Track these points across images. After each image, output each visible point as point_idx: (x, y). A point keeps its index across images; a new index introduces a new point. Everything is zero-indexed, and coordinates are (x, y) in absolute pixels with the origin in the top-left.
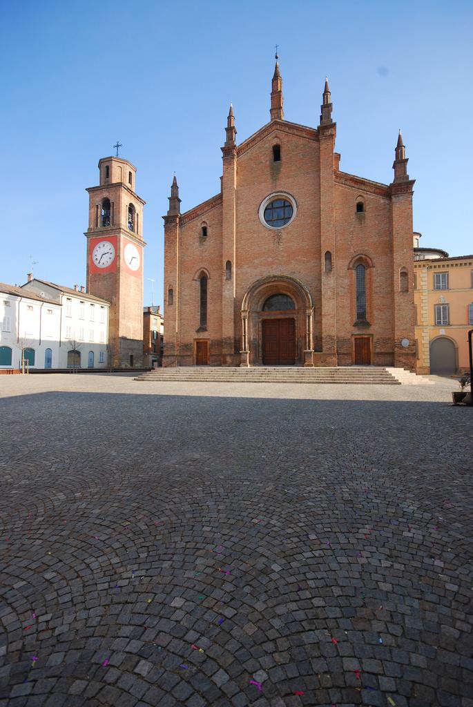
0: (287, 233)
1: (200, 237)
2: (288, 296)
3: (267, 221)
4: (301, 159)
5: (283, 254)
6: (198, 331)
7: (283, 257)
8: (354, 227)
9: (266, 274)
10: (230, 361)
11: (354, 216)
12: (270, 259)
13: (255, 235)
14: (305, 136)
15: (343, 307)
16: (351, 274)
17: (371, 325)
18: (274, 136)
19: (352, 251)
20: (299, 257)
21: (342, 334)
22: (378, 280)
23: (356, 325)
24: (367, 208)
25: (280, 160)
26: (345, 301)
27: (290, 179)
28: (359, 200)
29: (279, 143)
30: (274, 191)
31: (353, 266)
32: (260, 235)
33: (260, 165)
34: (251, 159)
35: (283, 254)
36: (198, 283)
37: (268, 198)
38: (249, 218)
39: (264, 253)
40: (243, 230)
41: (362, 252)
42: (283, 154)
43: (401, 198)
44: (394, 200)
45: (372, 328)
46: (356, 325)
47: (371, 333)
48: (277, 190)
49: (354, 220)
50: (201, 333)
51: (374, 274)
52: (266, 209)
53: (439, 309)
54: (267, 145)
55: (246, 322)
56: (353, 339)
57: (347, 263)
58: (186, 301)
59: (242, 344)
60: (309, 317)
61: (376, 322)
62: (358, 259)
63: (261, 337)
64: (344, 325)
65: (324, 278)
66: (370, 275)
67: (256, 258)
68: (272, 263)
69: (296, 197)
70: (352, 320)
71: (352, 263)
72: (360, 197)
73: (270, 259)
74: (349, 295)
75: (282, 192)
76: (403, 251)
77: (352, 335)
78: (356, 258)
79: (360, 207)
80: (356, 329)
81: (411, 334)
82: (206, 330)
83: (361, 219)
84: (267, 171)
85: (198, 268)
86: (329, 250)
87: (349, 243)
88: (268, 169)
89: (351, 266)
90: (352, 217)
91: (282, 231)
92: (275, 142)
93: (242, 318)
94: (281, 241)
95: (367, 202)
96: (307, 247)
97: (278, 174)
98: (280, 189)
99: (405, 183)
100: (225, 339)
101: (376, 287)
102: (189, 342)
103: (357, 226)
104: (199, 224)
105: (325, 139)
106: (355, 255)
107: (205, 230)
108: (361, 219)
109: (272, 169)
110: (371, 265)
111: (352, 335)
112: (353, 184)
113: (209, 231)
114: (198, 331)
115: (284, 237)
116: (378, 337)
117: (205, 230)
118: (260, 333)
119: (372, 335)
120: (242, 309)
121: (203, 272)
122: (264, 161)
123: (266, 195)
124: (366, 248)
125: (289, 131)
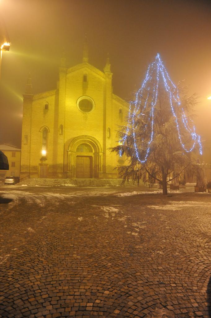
60: (101, 156)
69: (95, 100)
77: (117, 165)
85: (42, 125)
94: (87, 119)
111: (117, 165)
113: (50, 107)
117: (46, 107)
121: (45, 128)
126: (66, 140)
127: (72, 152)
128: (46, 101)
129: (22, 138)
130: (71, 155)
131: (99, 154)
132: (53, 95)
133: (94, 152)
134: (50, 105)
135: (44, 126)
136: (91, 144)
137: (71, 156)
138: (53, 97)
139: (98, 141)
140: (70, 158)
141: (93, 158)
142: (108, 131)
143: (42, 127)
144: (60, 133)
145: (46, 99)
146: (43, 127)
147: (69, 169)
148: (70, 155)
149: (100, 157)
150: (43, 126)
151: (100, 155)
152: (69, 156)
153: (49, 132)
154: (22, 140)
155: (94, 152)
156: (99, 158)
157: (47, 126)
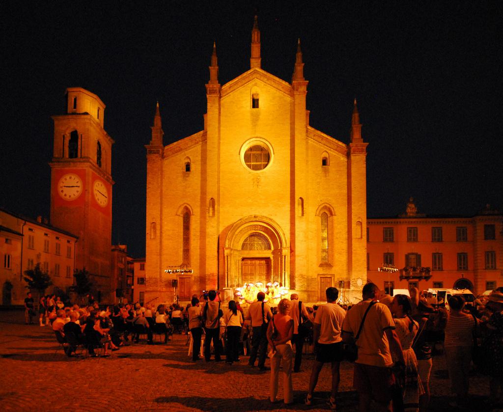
1: (183, 172)
2: (267, 240)
11: (320, 168)
12: (250, 201)
14: (282, 89)
17: (333, 266)
21: (310, 274)
22: (339, 227)
23: (321, 265)
24: (331, 162)
25: (258, 107)
28: (325, 155)
30: (253, 136)
31: (319, 214)
36: (181, 219)
43: (357, 157)
46: (321, 265)
48: (256, 136)
51: (335, 222)
53: (387, 256)
55: (229, 259)
56: (319, 277)
58: (169, 235)
59: (225, 282)
62: (323, 207)
66: (332, 222)
69: (273, 145)
71: (318, 211)
73: (250, 201)
75: (261, 138)
77: (318, 275)
78: (322, 206)
79: (325, 162)
80: (321, 269)
85: (181, 203)
89: (318, 213)
91: (261, 175)
95: (330, 158)
97: (257, 120)
98: (259, 135)
105: (300, 95)
106: (321, 203)
110: (334, 214)
112: (320, 140)
116: (338, 277)
117: (188, 168)
119: (334, 275)
120: (227, 246)
121: (186, 208)
126: (221, 229)
127: (232, 250)
129: (147, 229)
130: (231, 257)
131: (281, 253)
132: (198, 143)
133: (272, 248)
134: (194, 162)
135: (185, 203)
136: (267, 234)
137: (229, 257)
138: (199, 147)
140: (227, 262)
141: (272, 262)
142: (299, 204)
143: (180, 206)
144: (211, 214)
145: (186, 152)
146: (183, 207)
148: (227, 256)
149: (283, 257)
150: (182, 205)
151: (283, 254)
152: (226, 257)
153: (193, 215)
154: (147, 232)
155: (272, 248)
156: (281, 258)
157: (189, 203)
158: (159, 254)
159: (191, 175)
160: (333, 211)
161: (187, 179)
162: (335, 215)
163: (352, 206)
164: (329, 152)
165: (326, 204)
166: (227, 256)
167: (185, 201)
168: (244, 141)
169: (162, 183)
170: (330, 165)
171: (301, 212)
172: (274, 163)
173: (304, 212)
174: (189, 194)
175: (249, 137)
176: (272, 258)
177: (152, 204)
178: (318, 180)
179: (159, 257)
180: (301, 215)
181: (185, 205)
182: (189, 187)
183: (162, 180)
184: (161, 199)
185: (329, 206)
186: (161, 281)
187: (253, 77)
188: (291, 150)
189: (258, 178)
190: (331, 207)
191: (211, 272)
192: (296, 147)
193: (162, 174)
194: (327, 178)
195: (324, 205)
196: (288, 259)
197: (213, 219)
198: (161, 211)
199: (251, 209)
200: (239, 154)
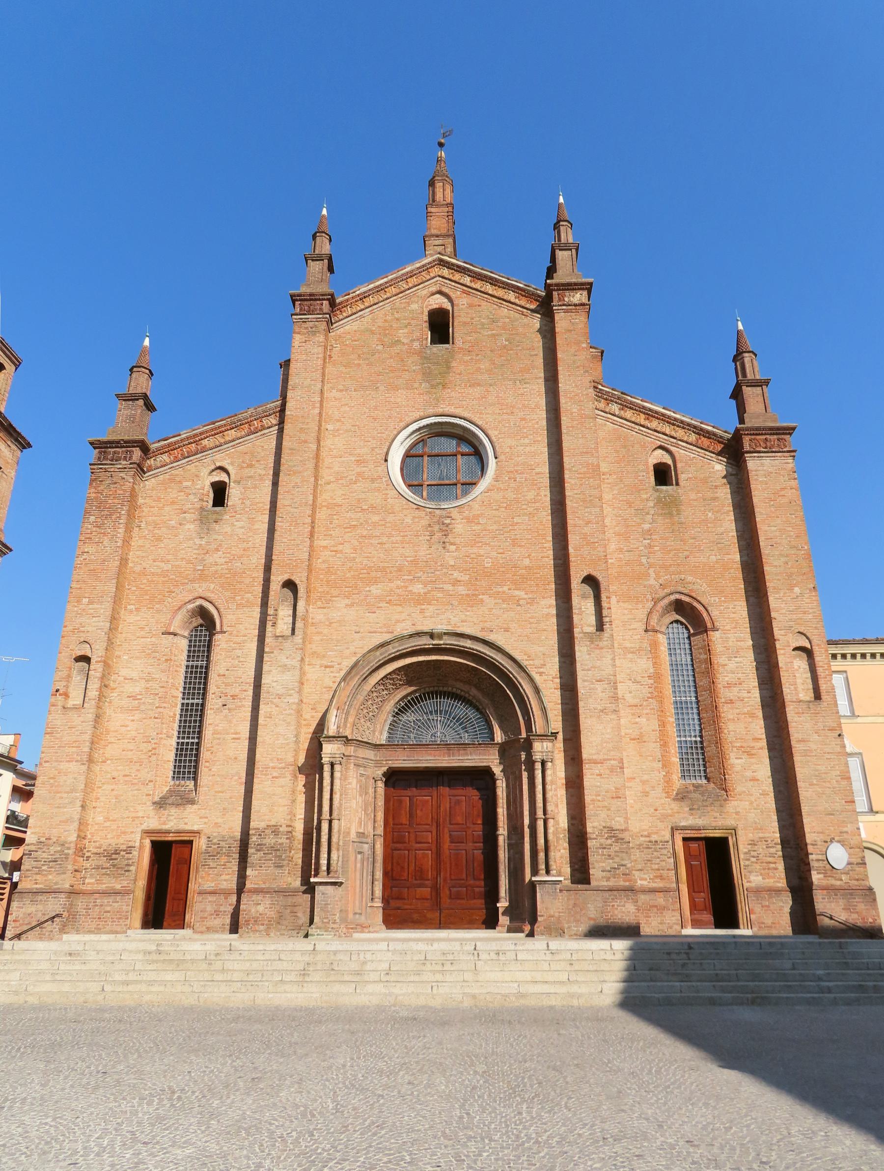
0: (469, 521)
3: (409, 486)
4: (505, 347)
5: (456, 574)
6: (161, 804)
7: (456, 582)
8: (654, 521)
9: (405, 628)
10: (272, 914)
12: (418, 588)
13: (375, 518)
14: (513, 300)
15: (639, 739)
16: (654, 645)
18: (434, 289)
19: (652, 582)
20: (505, 588)
22: (732, 665)
26: (643, 720)
27: (478, 389)
28: (661, 457)
29: (447, 305)
30: (431, 411)
32: (390, 518)
33: (397, 349)
34: (372, 332)
35: (456, 574)
37: (415, 426)
38: (359, 470)
39: (400, 570)
40: (339, 500)
41: (680, 589)
42: (458, 330)
44: (752, 464)
45: (732, 805)
46: (682, 796)
47: (730, 822)
48: (440, 411)
49: (651, 504)
50: (173, 811)
52: (408, 455)
54: (414, 306)
55: (337, 775)
57: (642, 614)
61: (739, 788)
62: (670, 604)
63: (380, 830)
64: (646, 794)
65: (581, 652)
67: (376, 581)
68: (421, 600)
69: (493, 433)
70: (668, 781)
72: (660, 451)
74: (654, 703)
76: (791, 589)
79: (663, 474)
81: (849, 828)
82: (192, 802)
83: (670, 507)
84: (413, 363)
86: (594, 573)
87: (644, 560)
88: (416, 358)
90: (645, 496)
91: (455, 513)
92: (438, 302)
93: (325, 760)
94: (450, 538)
95: (679, 465)
96: (527, 562)
99: (771, 429)
100: (261, 833)
101: (729, 686)
102: (121, 842)
103: (660, 519)
104: (205, 472)
105: (566, 311)
106: (662, 593)
107: (220, 493)
108: (670, 507)
109: (425, 358)
110: (709, 625)
111: (673, 830)
113: (234, 494)
114: (161, 804)
115: (459, 527)
117: (220, 493)
118: (380, 816)
121: (203, 613)
122: (405, 341)
123: (408, 420)
124: (690, 578)
125: (473, 285)
127: (347, 741)
128: (218, 464)
131: (529, 755)
137: (337, 768)
139: (524, 663)
146: (191, 606)
147: (324, 862)
148: (332, 765)
149: (538, 766)
151: (537, 757)
152: (327, 768)
153: (222, 632)
158: (85, 758)
159: (226, 517)
160: (705, 615)
161: (217, 527)
162: (715, 629)
163: (771, 599)
164: (673, 449)
165: (678, 596)
166: (332, 765)
167: (200, 592)
168: (402, 424)
169: (127, 541)
170: (681, 483)
171: (592, 620)
172: (496, 479)
173: (606, 620)
174: (214, 568)
175: (417, 415)
176: (497, 770)
177: (85, 601)
178: (647, 526)
179: (84, 768)
180: (593, 629)
181: (199, 602)
182: (217, 550)
183: (128, 529)
184: (119, 587)
185: (686, 599)
186: (80, 851)
187: (432, 275)
188: (549, 445)
189: (448, 521)
190: (695, 604)
191: (279, 817)
192: (565, 438)
193: (131, 516)
194: (676, 519)
195: (673, 597)
196: (557, 772)
197: (288, 644)
198: (114, 619)
199: (422, 611)
200: (386, 460)
